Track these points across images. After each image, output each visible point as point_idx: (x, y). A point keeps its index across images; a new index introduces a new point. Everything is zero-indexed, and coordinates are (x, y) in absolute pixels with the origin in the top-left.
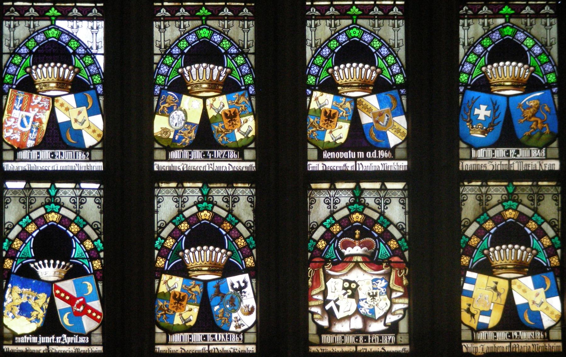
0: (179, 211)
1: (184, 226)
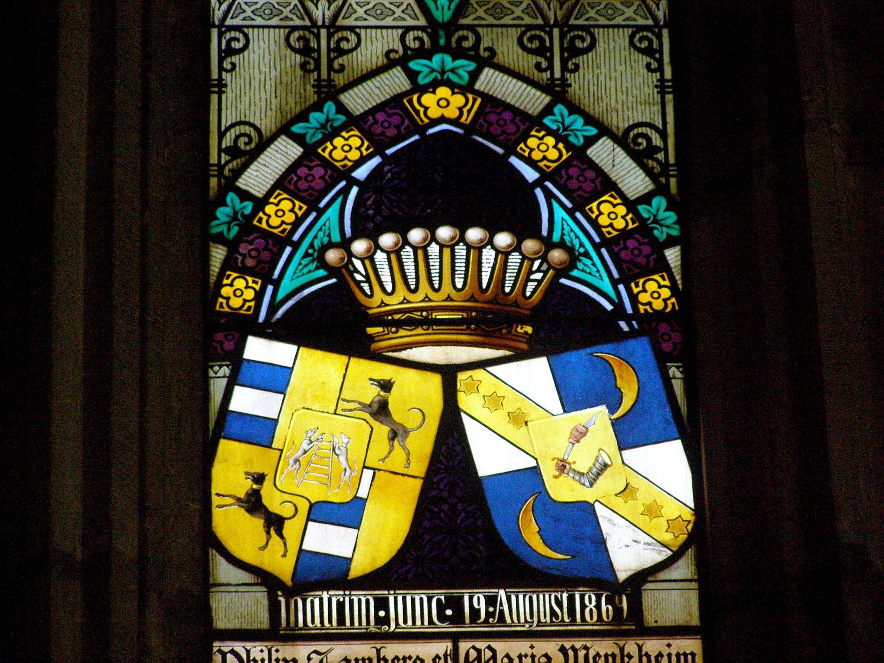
0: (318, 85)
1: (346, 148)
